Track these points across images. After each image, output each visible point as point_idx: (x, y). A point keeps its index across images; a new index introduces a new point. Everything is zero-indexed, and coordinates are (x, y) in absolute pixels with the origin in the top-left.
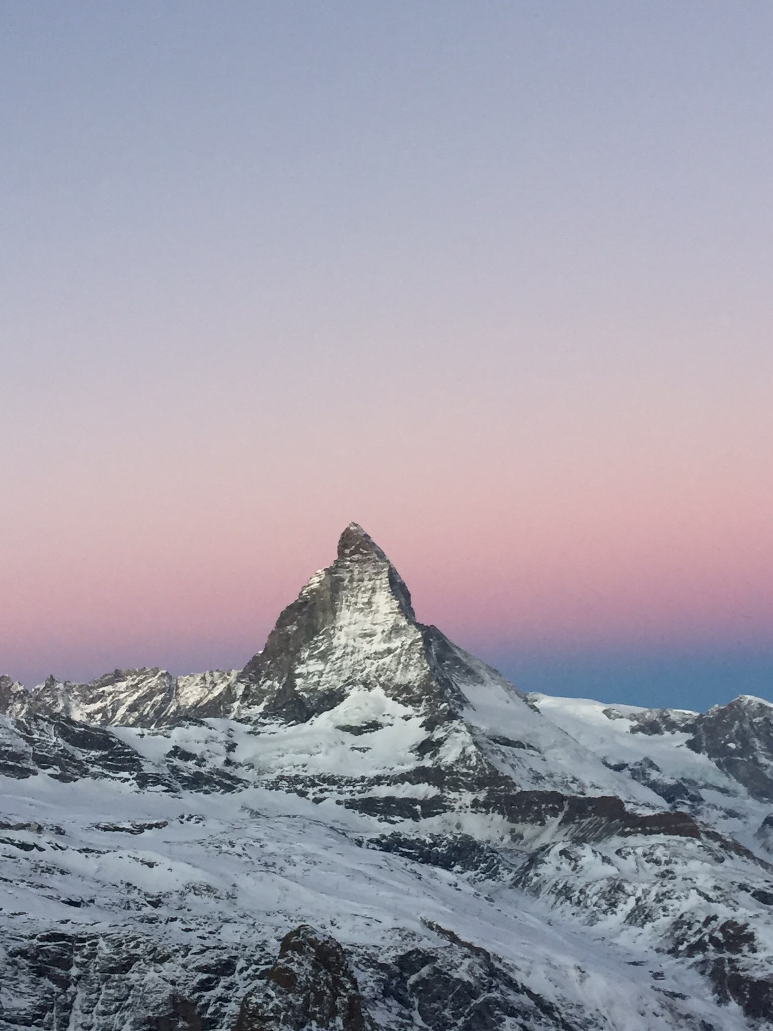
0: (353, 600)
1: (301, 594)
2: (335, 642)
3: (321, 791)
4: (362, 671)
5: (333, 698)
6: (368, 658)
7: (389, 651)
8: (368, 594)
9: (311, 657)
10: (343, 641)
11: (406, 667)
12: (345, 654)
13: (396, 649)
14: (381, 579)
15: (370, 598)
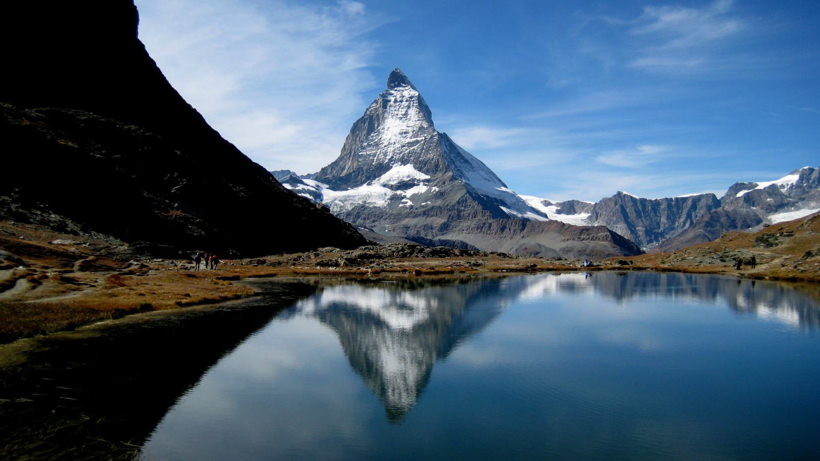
0: (396, 113)
1: (366, 112)
2: (384, 137)
3: (374, 221)
4: (400, 153)
5: (383, 168)
6: (404, 146)
7: (417, 142)
8: (405, 110)
9: (369, 145)
10: (389, 137)
11: (427, 151)
12: (389, 144)
13: (422, 140)
14: (414, 101)
15: (407, 111)
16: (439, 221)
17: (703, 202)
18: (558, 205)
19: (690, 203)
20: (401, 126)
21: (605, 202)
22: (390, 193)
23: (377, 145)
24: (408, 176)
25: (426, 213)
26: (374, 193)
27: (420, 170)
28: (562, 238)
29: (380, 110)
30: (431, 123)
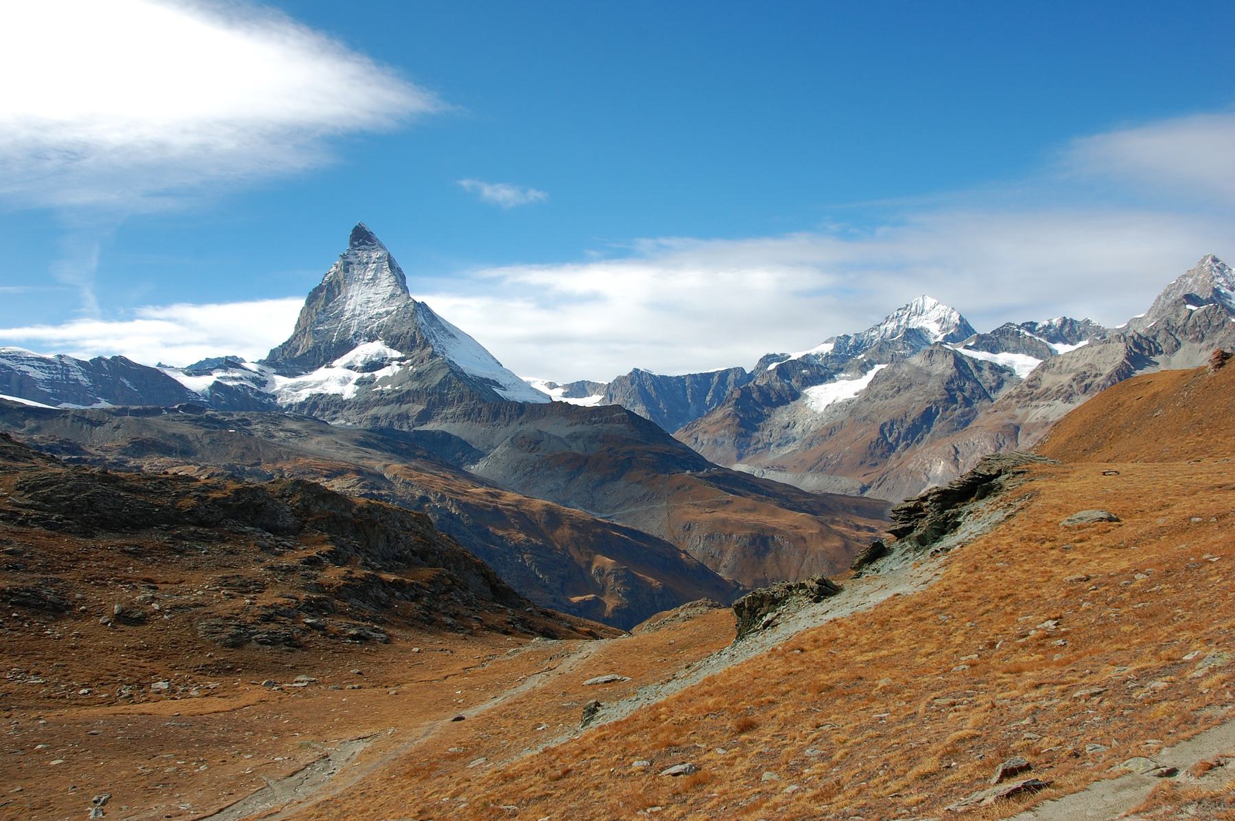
3: (335, 413)
5: (345, 346)
10: (352, 307)
12: (354, 315)
16: (417, 408)
17: (731, 377)
18: (565, 386)
19: (716, 378)
20: (370, 293)
21: (620, 380)
22: (356, 376)
23: (338, 317)
24: (378, 355)
25: (401, 398)
26: (334, 380)
27: (392, 346)
28: (569, 422)
29: (341, 275)
30: (405, 290)
